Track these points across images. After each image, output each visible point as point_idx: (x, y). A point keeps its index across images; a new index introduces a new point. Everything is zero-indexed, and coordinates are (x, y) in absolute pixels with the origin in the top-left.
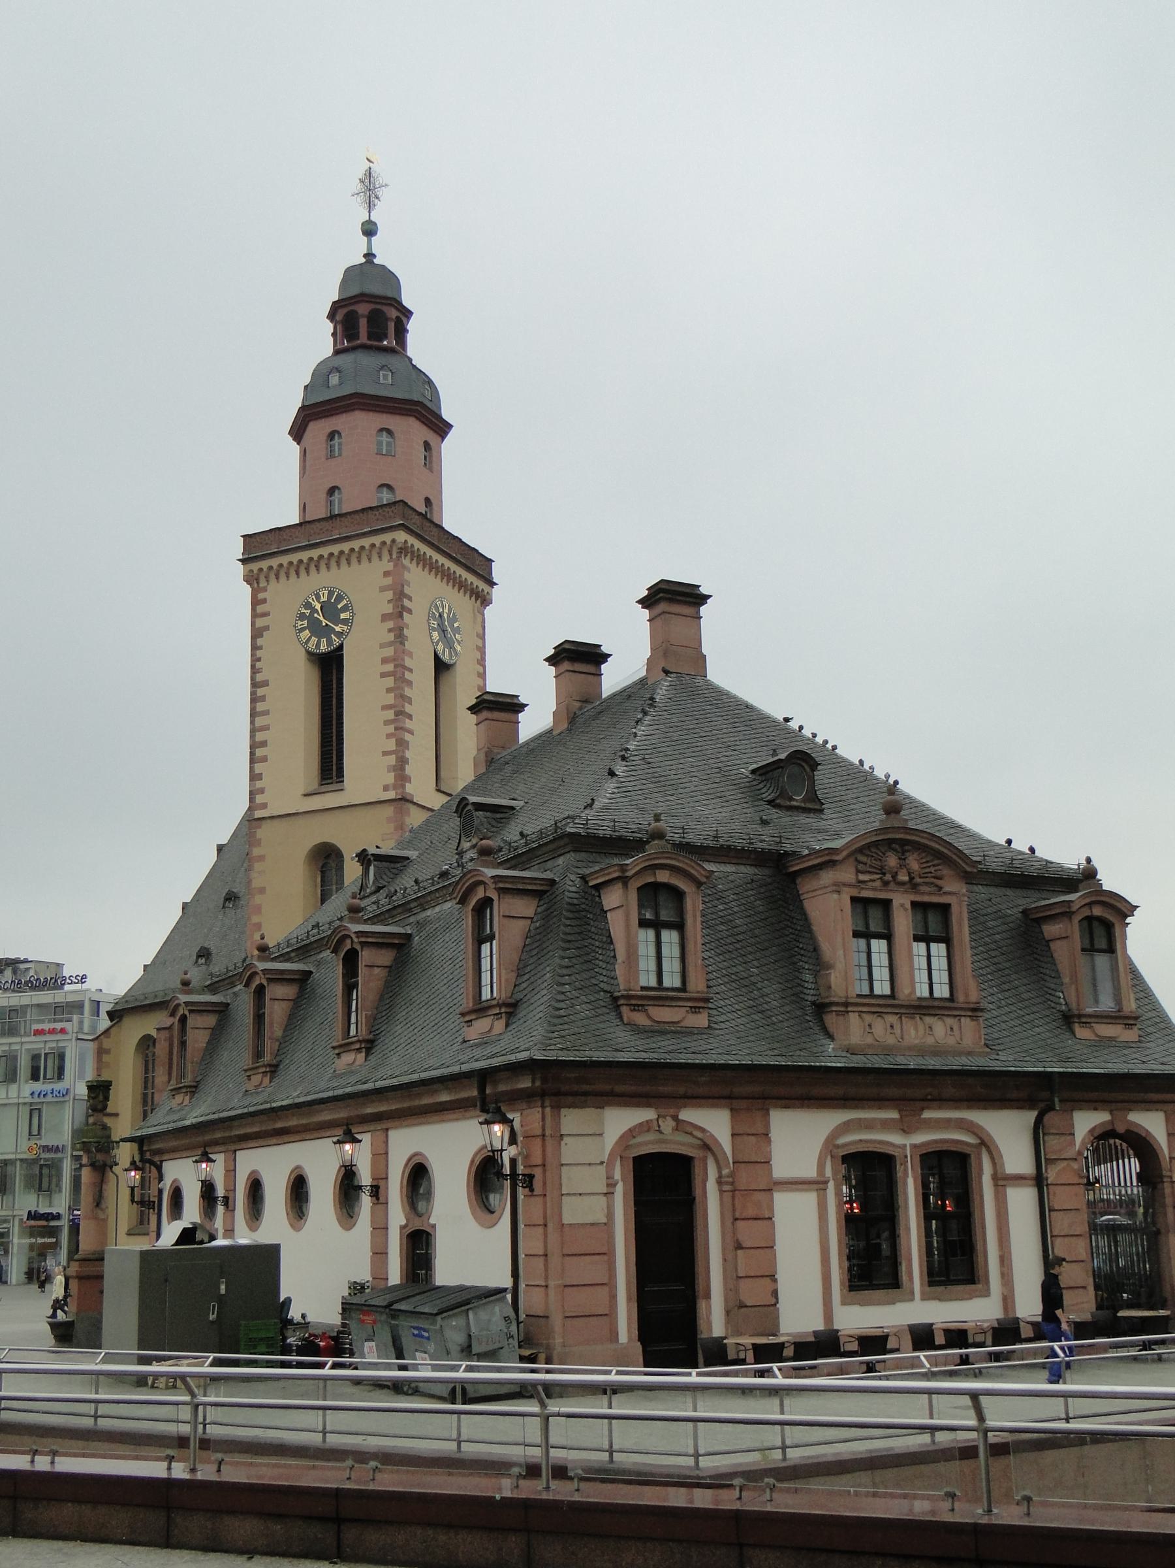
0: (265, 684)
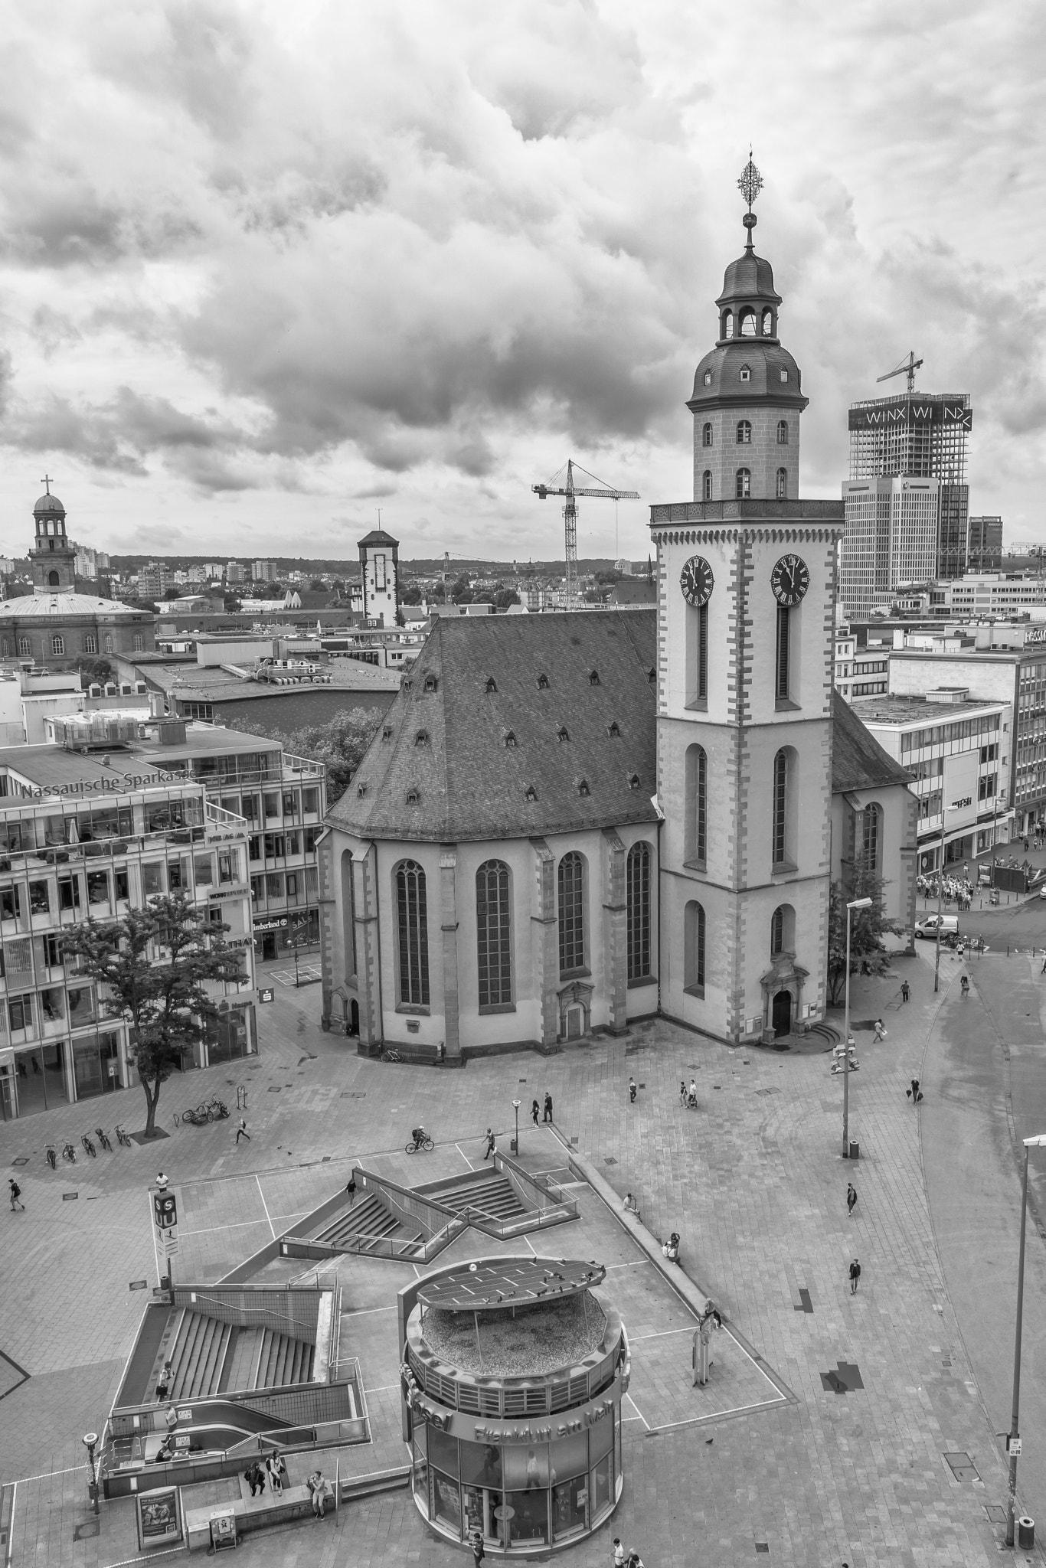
0: (750, 623)
